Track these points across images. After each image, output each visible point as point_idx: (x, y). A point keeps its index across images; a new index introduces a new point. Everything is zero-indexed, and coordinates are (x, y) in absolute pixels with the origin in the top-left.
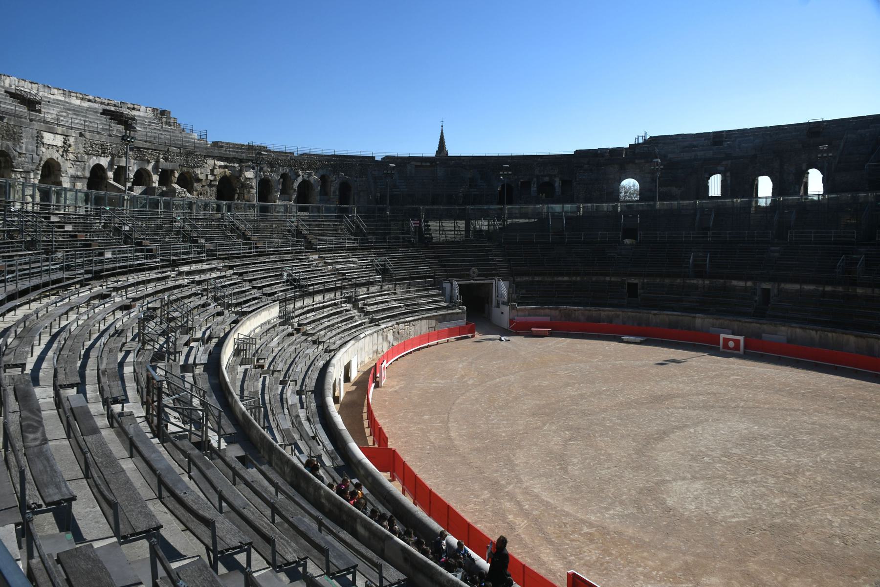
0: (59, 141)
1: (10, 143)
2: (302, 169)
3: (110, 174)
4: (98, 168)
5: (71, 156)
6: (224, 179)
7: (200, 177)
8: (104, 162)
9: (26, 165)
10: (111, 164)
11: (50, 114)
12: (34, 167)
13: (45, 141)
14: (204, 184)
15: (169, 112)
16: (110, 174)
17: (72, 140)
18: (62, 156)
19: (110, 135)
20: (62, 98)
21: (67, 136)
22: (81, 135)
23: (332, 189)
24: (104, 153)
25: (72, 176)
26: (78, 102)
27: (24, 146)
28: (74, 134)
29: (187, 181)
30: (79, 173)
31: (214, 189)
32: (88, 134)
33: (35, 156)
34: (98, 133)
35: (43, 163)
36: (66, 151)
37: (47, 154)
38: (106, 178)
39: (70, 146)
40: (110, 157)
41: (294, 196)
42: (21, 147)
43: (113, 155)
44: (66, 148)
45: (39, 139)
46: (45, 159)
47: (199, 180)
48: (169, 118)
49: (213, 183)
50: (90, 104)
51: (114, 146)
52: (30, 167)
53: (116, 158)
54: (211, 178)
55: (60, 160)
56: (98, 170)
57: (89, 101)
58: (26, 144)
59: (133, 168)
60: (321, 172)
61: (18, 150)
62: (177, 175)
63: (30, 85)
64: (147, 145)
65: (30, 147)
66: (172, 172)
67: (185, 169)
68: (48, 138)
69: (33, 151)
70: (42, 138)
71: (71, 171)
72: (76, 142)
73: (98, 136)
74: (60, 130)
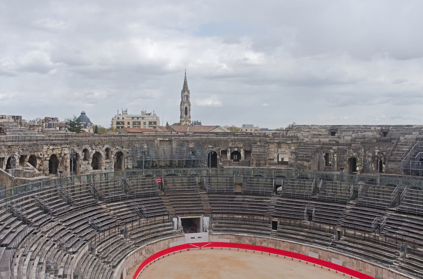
2: (96, 146)
6: (54, 156)
7: (40, 156)
14: (42, 160)
15: (21, 117)
23: (113, 156)
29: (33, 160)
31: (48, 162)
41: (91, 161)
47: (40, 158)
48: (21, 120)
49: (47, 159)
54: (46, 156)
60: (106, 146)
62: (28, 157)
66: (26, 156)
67: (33, 154)
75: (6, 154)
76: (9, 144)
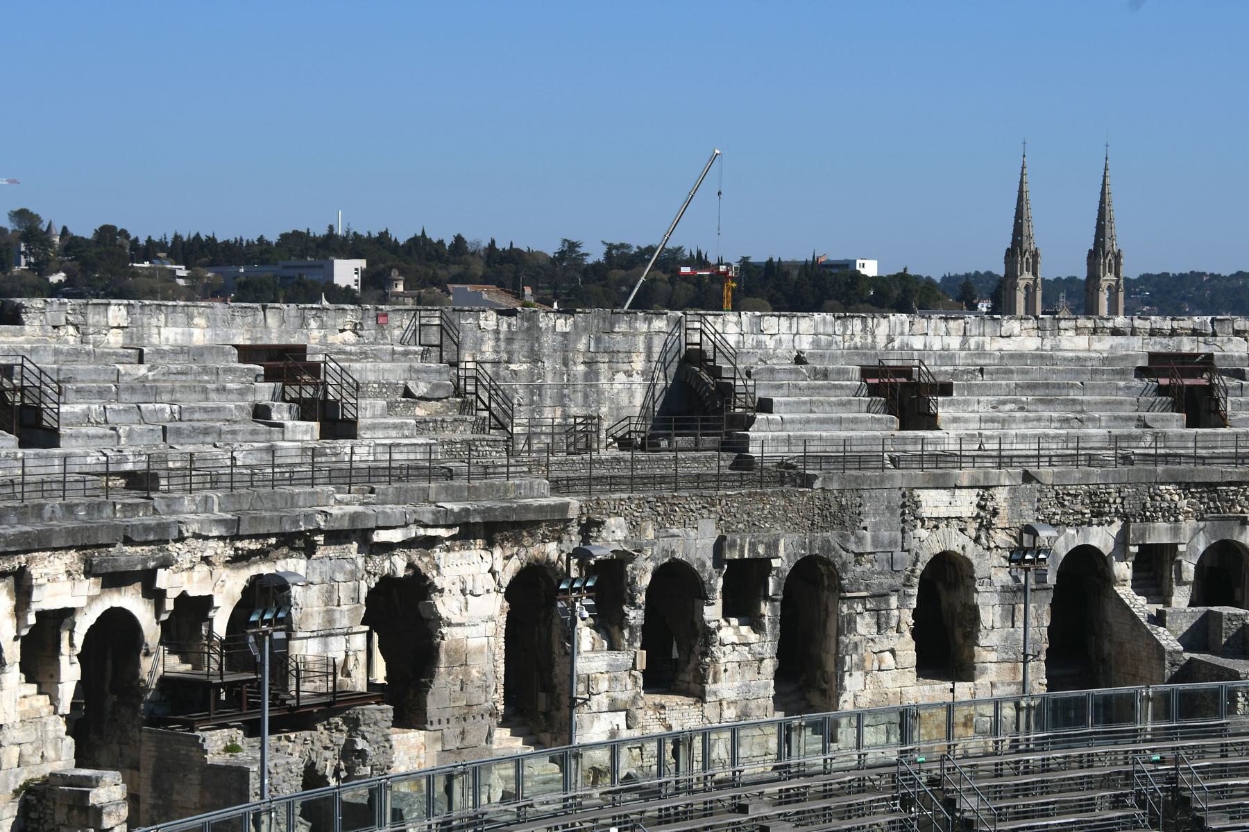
0: (965, 504)
1: (833, 536)
3: (1123, 570)
4: (1085, 557)
5: (1001, 538)
8: (1102, 537)
9: (875, 581)
10: (1122, 541)
11: (956, 424)
12: (899, 581)
13: (926, 511)
16: (1123, 570)
17: (1001, 497)
18: (977, 540)
19: (1126, 460)
20: (1030, 343)
21: (987, 488)
22: (1028, 477)
24: (1099, 514)
25: (1005, 589)
26: (1082, 342)
27: (868, 535)
28: (1007, 477)
32: (1046, 472)
33: (898, 553)
34: (1091, 460)
35: (920, 567)
36: (986, 527)
37: (929, 543)
38: (1108, 579)
40: (1118, 525)
42: (860, 541)
43: (1126, 518)
44: (985, 520)
45: (908, 512)
46: (926, 557)
51: (1128, 491)
52: (887, 581)
53: (1135, 525)
55: (972, 552)
56: (1085, 568)
57: (1116, 332)
58: (875, 528)
59: (1192, 543)
61: (853, 547)
63: (942, 325)
64: (1236, 472)
65: (885, 535)
68: (933, 502)
69: (893, 543)
70: (917, 505)
72: (1014, 501)
73: (1076, 473)
74: (964, 475)
75: (1188, 525)
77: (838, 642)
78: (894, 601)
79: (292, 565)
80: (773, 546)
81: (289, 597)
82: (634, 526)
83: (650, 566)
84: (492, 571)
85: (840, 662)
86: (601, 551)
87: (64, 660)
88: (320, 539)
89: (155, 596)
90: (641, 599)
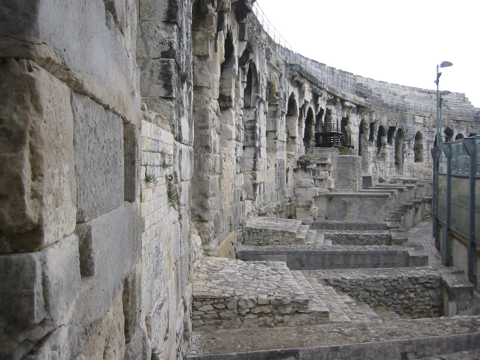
17: (427, 118)
30: (430, 139)
39: (426, 123)
50: (423, 93)
55: (422, 132)
71: (427, 138)
76: (459, 118)
77: (403, 151)
78: (411, 141)
79: (332, 108)
80: (397, 124)
81: (331, 117)
82: (376, 114)
83: (378, 126)
84: (358, 121)
85: (403, 156)
86: (374, 118)
87: (303, 120)
88: (339, 100)
89: (317, 105)
90: (377, 134)
